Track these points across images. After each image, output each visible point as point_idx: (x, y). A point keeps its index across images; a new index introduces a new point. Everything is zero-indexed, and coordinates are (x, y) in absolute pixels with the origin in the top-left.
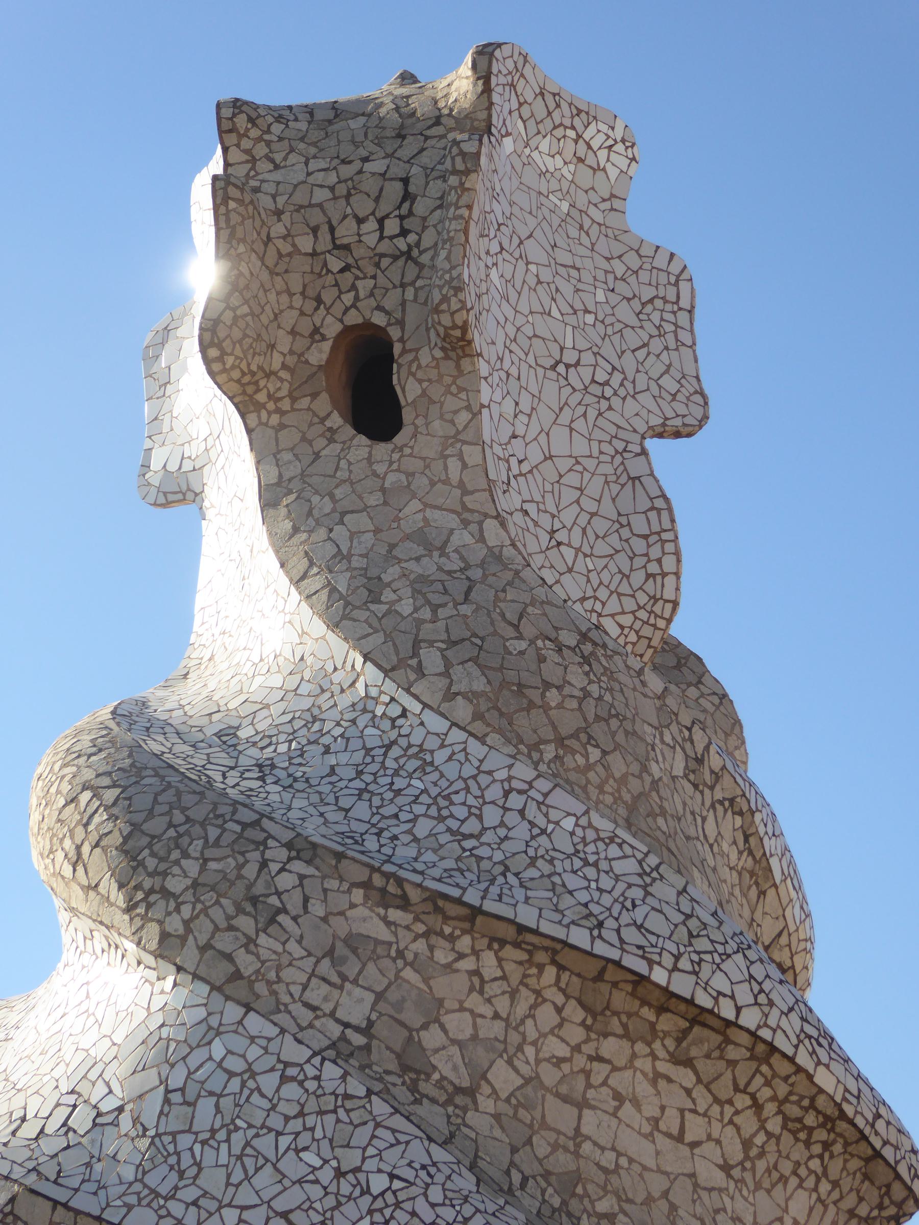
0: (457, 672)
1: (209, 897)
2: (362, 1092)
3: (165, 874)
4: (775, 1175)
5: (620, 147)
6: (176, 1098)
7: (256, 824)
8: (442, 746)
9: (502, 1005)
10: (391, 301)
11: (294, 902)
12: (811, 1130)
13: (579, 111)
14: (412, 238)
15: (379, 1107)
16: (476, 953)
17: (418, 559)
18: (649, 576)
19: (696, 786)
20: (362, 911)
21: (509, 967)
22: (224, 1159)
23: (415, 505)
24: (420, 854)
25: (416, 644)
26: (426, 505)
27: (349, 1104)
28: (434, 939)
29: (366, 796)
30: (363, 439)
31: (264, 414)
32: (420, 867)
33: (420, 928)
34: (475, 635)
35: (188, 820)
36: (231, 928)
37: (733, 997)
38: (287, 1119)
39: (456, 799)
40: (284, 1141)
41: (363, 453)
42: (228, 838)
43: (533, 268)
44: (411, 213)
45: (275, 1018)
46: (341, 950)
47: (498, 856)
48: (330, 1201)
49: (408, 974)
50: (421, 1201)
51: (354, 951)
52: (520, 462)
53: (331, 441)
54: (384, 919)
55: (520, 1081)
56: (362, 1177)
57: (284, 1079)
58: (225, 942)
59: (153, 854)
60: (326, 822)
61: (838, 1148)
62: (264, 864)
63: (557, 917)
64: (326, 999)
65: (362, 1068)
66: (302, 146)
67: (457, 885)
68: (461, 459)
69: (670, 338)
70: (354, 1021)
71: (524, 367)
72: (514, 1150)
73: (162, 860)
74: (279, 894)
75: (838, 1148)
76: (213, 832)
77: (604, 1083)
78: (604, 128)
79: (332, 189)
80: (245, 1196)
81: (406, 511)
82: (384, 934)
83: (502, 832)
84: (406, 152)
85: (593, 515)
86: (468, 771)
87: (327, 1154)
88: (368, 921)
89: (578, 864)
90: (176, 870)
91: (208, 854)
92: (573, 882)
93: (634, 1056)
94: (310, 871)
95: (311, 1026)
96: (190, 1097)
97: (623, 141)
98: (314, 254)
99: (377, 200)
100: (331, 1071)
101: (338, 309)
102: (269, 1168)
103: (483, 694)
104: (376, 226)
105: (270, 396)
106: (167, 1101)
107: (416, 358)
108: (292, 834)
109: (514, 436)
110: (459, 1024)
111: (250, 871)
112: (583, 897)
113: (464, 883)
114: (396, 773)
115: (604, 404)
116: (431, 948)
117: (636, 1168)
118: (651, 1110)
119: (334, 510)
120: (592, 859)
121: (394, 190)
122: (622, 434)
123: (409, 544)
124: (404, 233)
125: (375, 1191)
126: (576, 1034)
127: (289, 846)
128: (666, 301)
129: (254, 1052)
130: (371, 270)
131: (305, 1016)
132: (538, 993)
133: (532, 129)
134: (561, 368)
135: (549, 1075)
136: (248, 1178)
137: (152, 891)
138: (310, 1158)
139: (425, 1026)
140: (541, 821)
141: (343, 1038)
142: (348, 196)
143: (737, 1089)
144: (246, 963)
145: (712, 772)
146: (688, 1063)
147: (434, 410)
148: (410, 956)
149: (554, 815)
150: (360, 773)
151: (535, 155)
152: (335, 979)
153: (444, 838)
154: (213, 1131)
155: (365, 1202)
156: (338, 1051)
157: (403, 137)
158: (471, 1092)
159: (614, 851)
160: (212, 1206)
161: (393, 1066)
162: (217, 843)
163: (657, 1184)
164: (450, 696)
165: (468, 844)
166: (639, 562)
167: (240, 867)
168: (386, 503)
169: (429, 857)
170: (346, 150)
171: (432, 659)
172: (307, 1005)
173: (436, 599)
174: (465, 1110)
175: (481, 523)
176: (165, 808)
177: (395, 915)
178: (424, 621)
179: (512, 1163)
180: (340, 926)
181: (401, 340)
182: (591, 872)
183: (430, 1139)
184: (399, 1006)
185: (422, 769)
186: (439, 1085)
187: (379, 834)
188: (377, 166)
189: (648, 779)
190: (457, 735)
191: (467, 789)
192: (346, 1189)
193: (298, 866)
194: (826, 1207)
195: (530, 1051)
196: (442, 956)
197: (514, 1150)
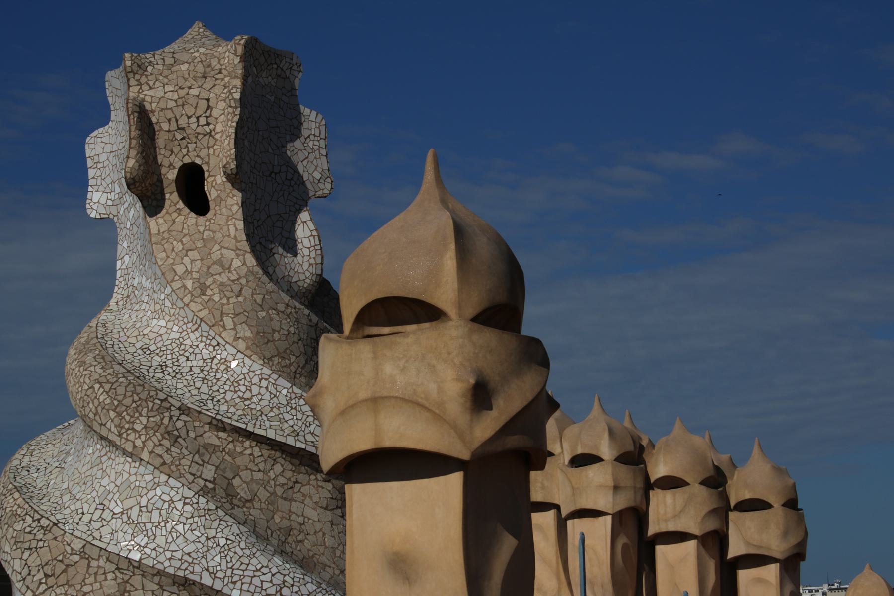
0: (239, 327)
1: (151, 432)
2: (214, 507)
3: (133, 423)
6: (144, 509)
7: (166, 399)
8: (234, 359)
10: (203, 153)
11: (183, 433)
14: (211, 127)
15: (221, 513)
17: (220, 274)
18: (310, 265)
22: (164, 533)
23: (217, 247)
24: (229, 409)
25: (222, 314)
26: (221, 247)
27: (210, 513)
28: (236, 443)
29: (205, 382)
30: (193, 214)
31: (150, 201)
32: (230, 415)
33: (231, 439)
34: (245, 311)
35: (140, 399)
36: (161, 445)
38: (187, 519)
39: (242, 383)
40: (187, 527)
41: (193, 221)
42: (156, 407)
43: (261, 133)
44: (210, 115)
45: (180, 480)
46: (202, 450)
47: (259, 408)
48: (205, 549)
49: (227, 458)
50: (238, 548)
51: (207, 450)
53: (180, 214)
54: (217, 436)
55: (269, 495)
56: (216, 540)
57: (185, 504)
58: (159, 450)
59: (128, 414)
60: (192, 395)
62: (171, 418)
63: (281, 433)
64: (198, 471)
65: (212, 497)
66: (161, 78)
67: (244, 423)
68: (235, 226)
69: (317, 153)
70: (209, 479)
72: (268, 521)
73: (131, 417)
74: (177, 430)
76: (150, 405)
77: (299, 491)
78: (288, 60)
79: (176, 101)
80: (173, 547)
81: (214, 250)
82: (217, 442)
83: (259, 397)
84: (207, 86)
85: (287, 239)
86: (245, 371)
87: (203, 532)
88: (211, 438)
89: (289, 409)
90: (138, 421)
91: (150, 414)
92: (287, 417)
94: (188, 419)
95: (193, 482)
96: (150, 509)
98: (169, 131)
99: (196, 108)
100: (202, 500)
101: (180, 156)
102: (181, 537)
103: (249, 338)
104: (195, 120)
105: (153, 193)
106: (140, 510)
107: (215, 180)
108: (180, 404)
109: (255, 210)
110: (245, 475)
112: (291, 423)
113: (246, 421)
114: (216, 371)
115: (291, 189)
116: (235, 446)
117: (311, 521)
118: (316, 499)
119: (183, 249)
120: (294, 406)
121: (203, 104)
123: (215, 266)
124: (208, 124)
125: (221, 545)
126: (288, 474)
127: (179, 409)
129: (173, 493)
130: (194, 140)
131: (191, 478)
132: (275, 460)
134: (273, 175)
135: (279, 491)
136: (174, 540)
137: (128, 429)
138: (197, 533)
139: (234, 478)
140: (274, 391)
141: (205, 486)
142: (183, 105)
144: (168, 458)
147: (223, 203)
148: (227, 450)
149: (279, 389)
150: (202, 370)
151: (261, 80)
152: (201, 463)
153: (238, 400)
154: (160, 523)
155: (218, 548)
156: (203, 492)
157: (206, 78)
160: (161, 550)
161: (224, 495)
162: (152, 410)
164: (236, 339)
165: (247, 403)
166: (306, 259)
167: (162, 419)
168: (205, 246)
169: (232, 410)
170: (181, 82)
171: (228, 322)
172: (191, 474)
173: (229, 294)
174: (250, 508)
175: (244, 256)
176: (130, 394)
177: (221, 434)
178: (224, 305)
181: (208, 171)
182: (293, 412)
184: (224, 471)
185: (226, 369)
186: (240, 500)
187: (212, 400)
188: (195, 92)
190: (240, 355)
191: (245, 378)
192: (210, 544)
193: (183, 417)
196: (239, 449)
197: (268, 521)
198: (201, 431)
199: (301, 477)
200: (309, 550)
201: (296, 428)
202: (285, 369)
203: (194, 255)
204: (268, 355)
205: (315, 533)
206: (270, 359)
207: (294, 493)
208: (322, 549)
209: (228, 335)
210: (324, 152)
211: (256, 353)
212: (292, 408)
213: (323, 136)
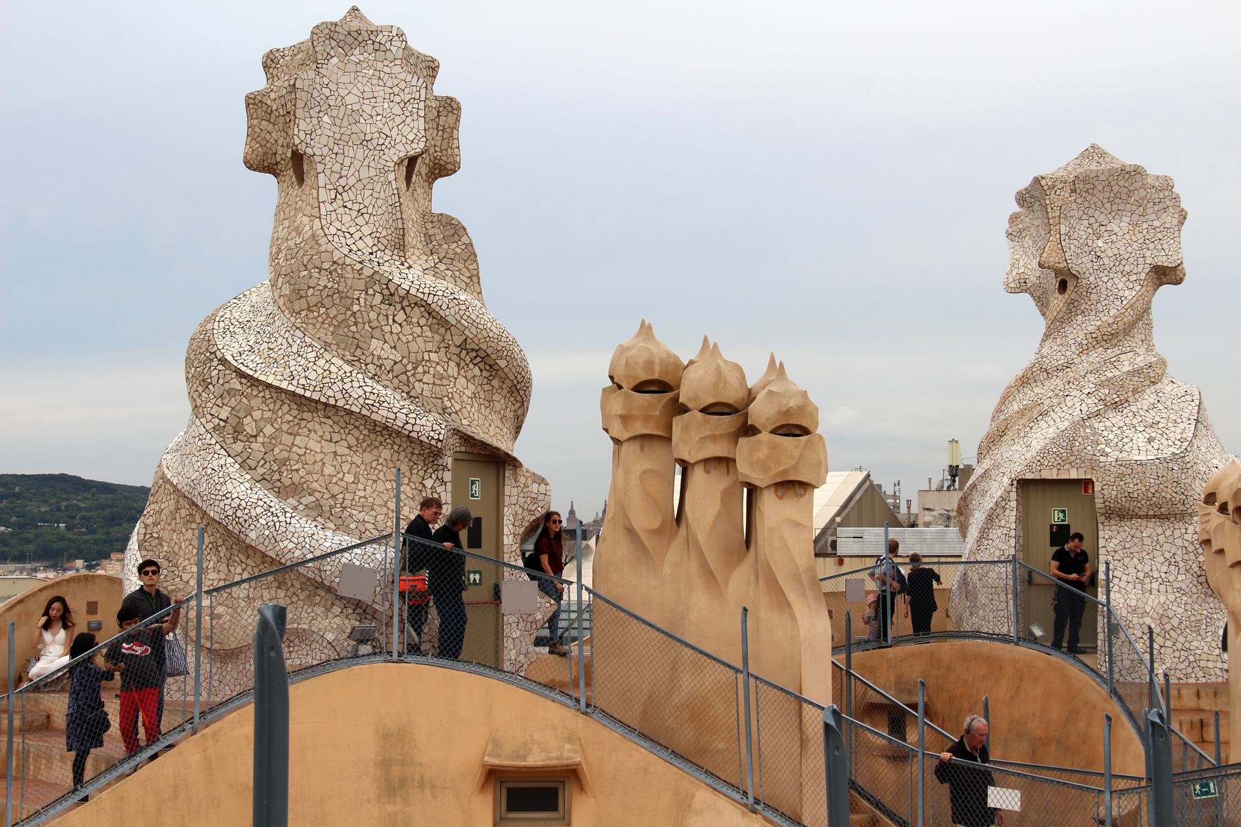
9: (271, 406)
15: (218, 447)
49: (244, 400)
82: (238, 387)
92: (292, 363)
110: (257, 414)
126: (295, 412)
131: (209, 417)
133: (347, 48)
135: (285, 427)
158: (255, 436)
163: (319, 457)
177: (244, 381)
180: (227, 386)
189: (349, 313)
193: (220, 367)
196: (255, 393)
203: (286, 223)
204: (297, 309)
210: (422, 113)
213: (423, 98)
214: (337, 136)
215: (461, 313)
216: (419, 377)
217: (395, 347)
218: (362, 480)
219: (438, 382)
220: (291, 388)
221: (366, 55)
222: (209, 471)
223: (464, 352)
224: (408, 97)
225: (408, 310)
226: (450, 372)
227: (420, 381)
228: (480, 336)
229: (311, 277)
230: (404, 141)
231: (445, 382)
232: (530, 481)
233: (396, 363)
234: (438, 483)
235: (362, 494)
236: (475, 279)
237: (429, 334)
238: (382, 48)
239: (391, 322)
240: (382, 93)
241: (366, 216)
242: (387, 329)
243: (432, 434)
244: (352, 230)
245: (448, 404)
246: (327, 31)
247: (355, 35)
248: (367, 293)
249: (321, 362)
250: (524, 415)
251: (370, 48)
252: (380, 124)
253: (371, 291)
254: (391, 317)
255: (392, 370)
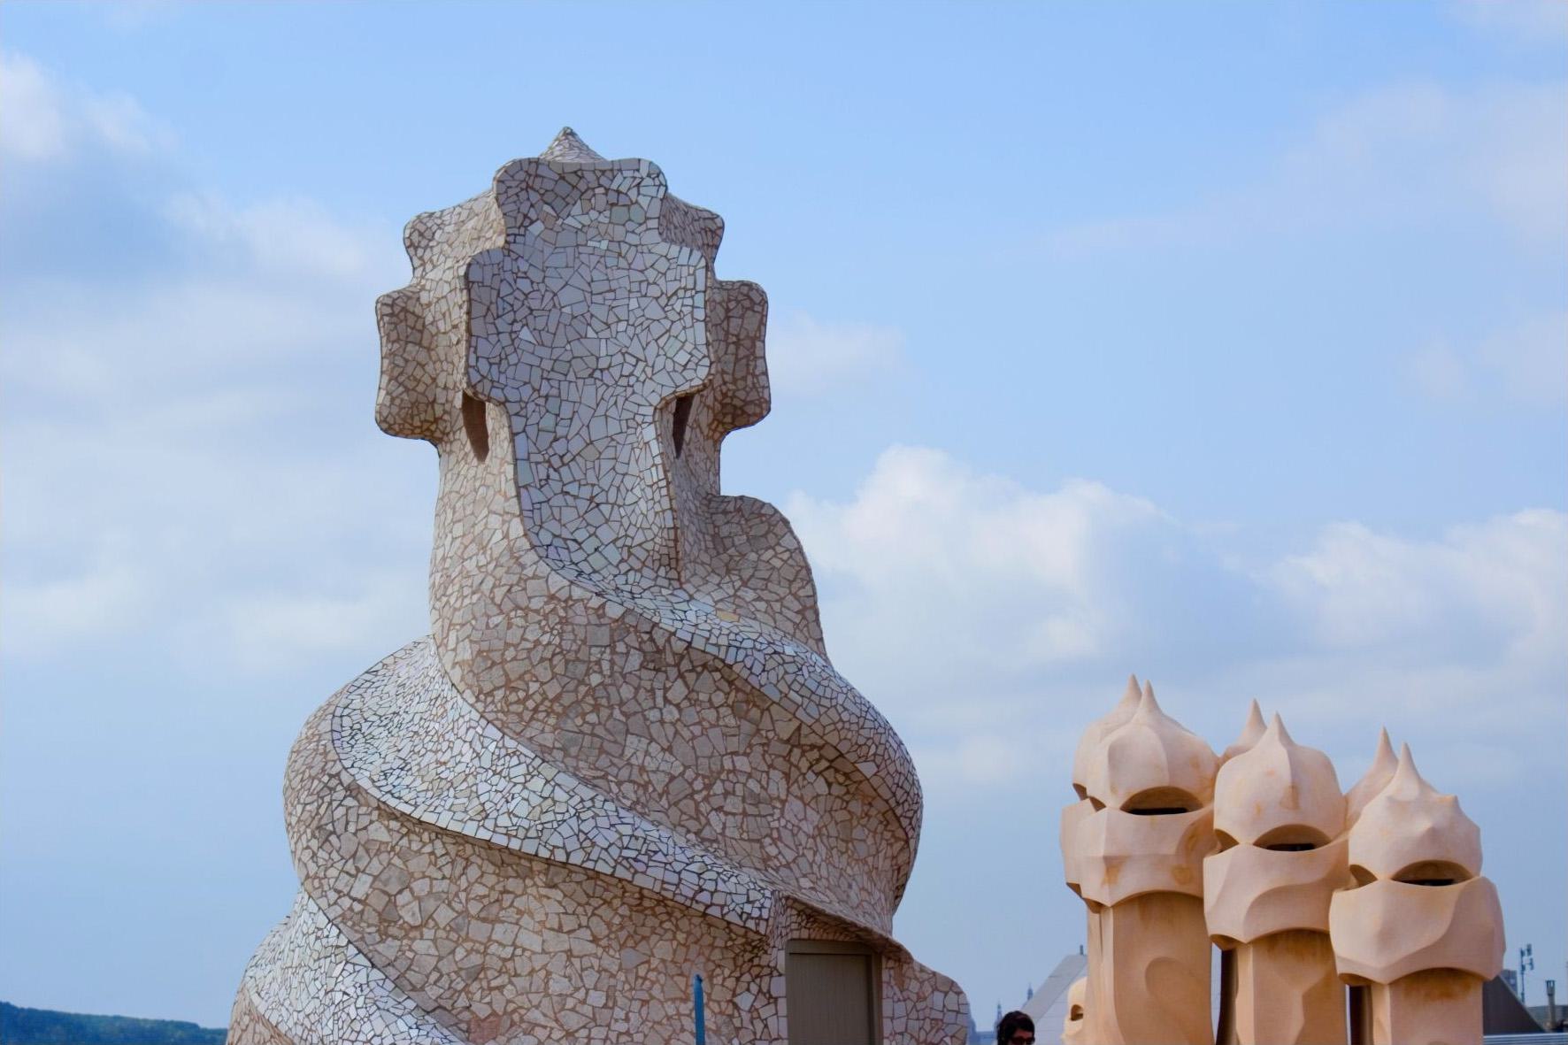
4: (638, 938)
5: (648, 181)
7: (338, 774)
9: (447, 871)
11: (340, 828)
12: (652, 909)
13: (603, 172)
15: (352, 950)
16: (431, 841)
19: (657, 670)
20: (377, 824)
21: (450, 847)
28: (413, 837)
33: (404, 830)
37: (564, 847)
41: (472, 472)
43: (567, 310)
46: (361, 851)
49: (396, 861)
51: (367, 851)
52: (561, 457)
54: (387, 827)
61: (677, 914)
62: (330, 804)
69: (688, 320)
71: (564, 385)
75: (677, 914)
77: (511, 905)
82: (383, 836)
88: (379, 832)
92: (483, 787)
93: (526, 887)
94: (355, 803)
97: (649, 175)
109: (556, 439)
110: (420, 887)
111: (322, 811)
112: (483, 799)
115: (630, 390)
117: (527, 954)
118: (540, 917)
122: (642, 410)
126: (491, 880)
127: (347, 789)
128: (686, 289)
131: (333, 896)
132: (467, 859)
133: (559, 203)
134: (597, 374)
135: (474, 908)
139: (400, 892)
140: (478, 748)
141: (351, 909)
143: (588, 896)
145: (674, 654)
146: (555, 886)
149: (487, 741)
159: (515, 761)
163: (539, 962)
174: (413, 940)
177: (394, 825)
179: (436, 968)
183: (373, 966)
184: (386, 883)
189: (583, 689)
193: (350, 802)
194: (688, 947)
195: (463, 896)
196: (415, 846)
197: (440, 958)
198: (364, 821)
199: (512, 884)
200: (509, 1001)
201: (487, 806)
202: (513, 708)
203: (458, 530)
204: (487, 687)
205: (532, 972)
206: (490, 694)
207: (503, 909)
208: (535, 999)
209: (448, 658)
210: (700, 314)
211: (470, 687)
212: (495, 773)
213: (700, 287)
214: (547, 365)
215: (789, 678)
216: (716, 802)
217: (669, 749)
218: (621, 1001)
219: (751, 810)
220: (484, 835)
221: (594, 214)
222: (338, 997)
223: (797, 752)
224: (676, 285)
225: (691, 677)
226: (773, 789)
227: (720, 809)
228: (825, 720)
229: (509, 626)
230: (670, 366)
231: (764, 809)
232: (927, 989)
233: (672, 778)
234: (762, 1000)
235: (622, 1027)
236: (810, 615)
237: (732, 721)
238: (623, 200)
239: (660, 701)
240: (625, 283)
241: (605, 509)
242: (653, 715)
243: (748, 908)
244: (581, 535)
245: (772, 851)
246: (522, 175)
247: (573, 179)
248: (613, 652)
249: (537, 784)
250: (909, 864)
251: (600, 201)
252: (624, 339)
253: (621, 648)
254: (659, 694)
255: (666, 792)
